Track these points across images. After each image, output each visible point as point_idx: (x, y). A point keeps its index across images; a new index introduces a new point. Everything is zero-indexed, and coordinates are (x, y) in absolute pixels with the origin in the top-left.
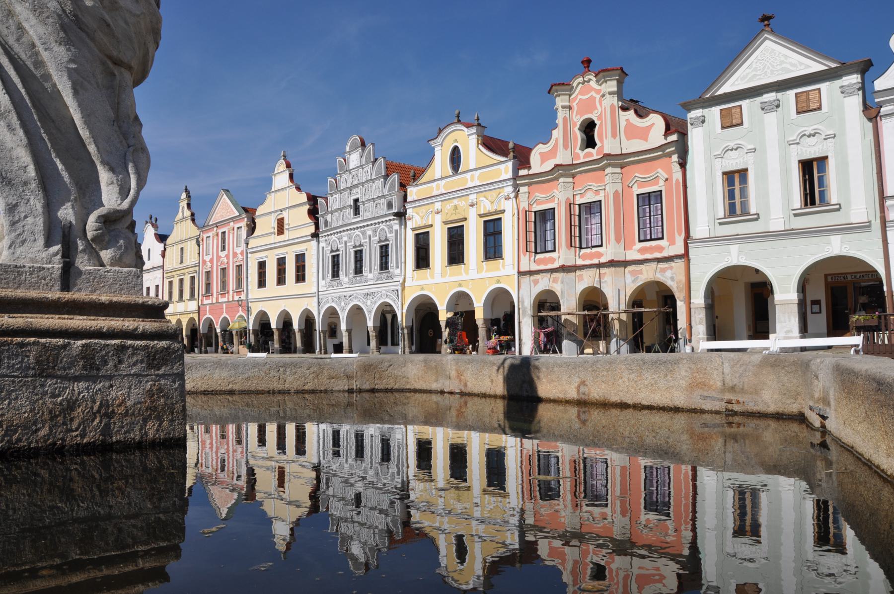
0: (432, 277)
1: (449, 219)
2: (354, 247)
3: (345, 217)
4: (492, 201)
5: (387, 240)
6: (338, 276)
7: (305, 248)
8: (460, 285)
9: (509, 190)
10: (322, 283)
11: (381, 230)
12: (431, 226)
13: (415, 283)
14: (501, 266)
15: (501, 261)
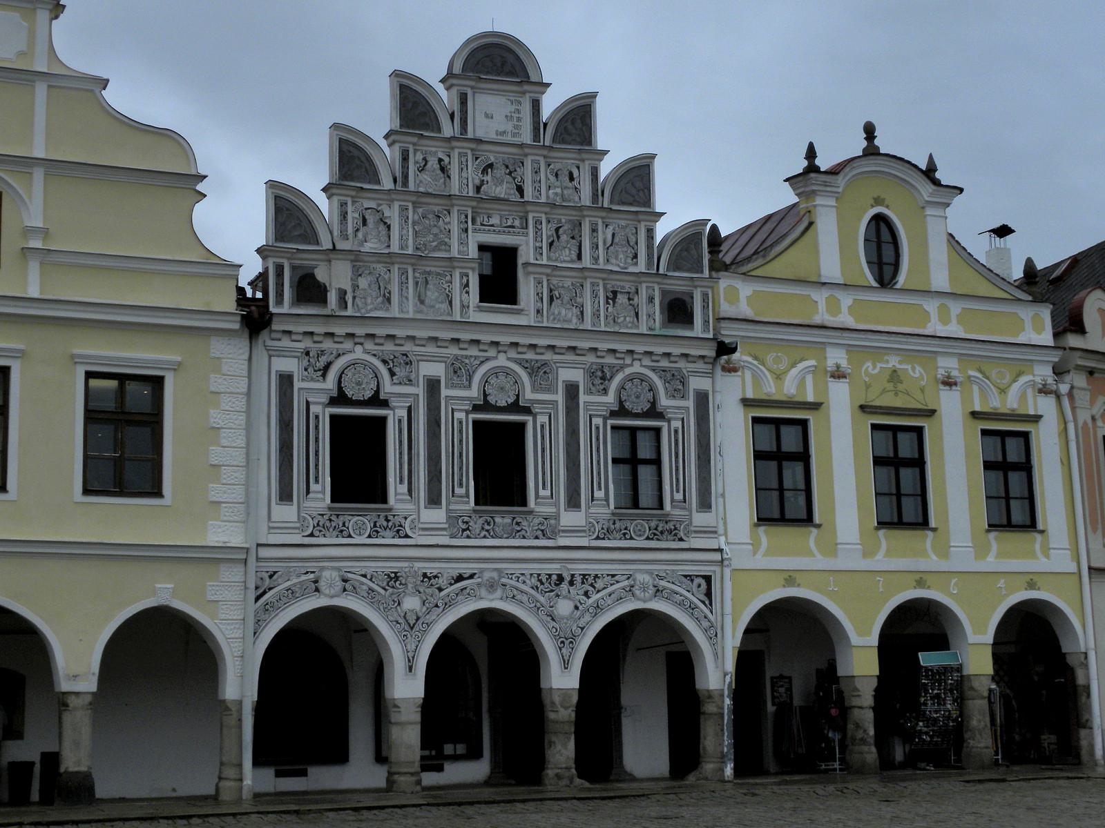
0: (831, 548)
1: (877, 403)
2: (476, 408)
3: (432, 295)
4: (1001, 386)
5: (653, 412)
6: (377, 493)
7: (179, 359)
8: (920, 583)
9: (1044, 373)
10: (286, 513)
11: (630, 379)
12: (815, 406)
13: (761, 561)
14: (1037, 546)
15: (1038, 537)
